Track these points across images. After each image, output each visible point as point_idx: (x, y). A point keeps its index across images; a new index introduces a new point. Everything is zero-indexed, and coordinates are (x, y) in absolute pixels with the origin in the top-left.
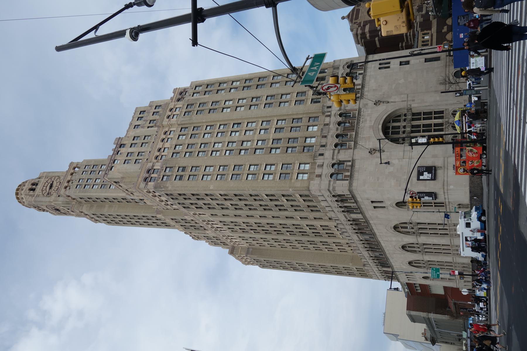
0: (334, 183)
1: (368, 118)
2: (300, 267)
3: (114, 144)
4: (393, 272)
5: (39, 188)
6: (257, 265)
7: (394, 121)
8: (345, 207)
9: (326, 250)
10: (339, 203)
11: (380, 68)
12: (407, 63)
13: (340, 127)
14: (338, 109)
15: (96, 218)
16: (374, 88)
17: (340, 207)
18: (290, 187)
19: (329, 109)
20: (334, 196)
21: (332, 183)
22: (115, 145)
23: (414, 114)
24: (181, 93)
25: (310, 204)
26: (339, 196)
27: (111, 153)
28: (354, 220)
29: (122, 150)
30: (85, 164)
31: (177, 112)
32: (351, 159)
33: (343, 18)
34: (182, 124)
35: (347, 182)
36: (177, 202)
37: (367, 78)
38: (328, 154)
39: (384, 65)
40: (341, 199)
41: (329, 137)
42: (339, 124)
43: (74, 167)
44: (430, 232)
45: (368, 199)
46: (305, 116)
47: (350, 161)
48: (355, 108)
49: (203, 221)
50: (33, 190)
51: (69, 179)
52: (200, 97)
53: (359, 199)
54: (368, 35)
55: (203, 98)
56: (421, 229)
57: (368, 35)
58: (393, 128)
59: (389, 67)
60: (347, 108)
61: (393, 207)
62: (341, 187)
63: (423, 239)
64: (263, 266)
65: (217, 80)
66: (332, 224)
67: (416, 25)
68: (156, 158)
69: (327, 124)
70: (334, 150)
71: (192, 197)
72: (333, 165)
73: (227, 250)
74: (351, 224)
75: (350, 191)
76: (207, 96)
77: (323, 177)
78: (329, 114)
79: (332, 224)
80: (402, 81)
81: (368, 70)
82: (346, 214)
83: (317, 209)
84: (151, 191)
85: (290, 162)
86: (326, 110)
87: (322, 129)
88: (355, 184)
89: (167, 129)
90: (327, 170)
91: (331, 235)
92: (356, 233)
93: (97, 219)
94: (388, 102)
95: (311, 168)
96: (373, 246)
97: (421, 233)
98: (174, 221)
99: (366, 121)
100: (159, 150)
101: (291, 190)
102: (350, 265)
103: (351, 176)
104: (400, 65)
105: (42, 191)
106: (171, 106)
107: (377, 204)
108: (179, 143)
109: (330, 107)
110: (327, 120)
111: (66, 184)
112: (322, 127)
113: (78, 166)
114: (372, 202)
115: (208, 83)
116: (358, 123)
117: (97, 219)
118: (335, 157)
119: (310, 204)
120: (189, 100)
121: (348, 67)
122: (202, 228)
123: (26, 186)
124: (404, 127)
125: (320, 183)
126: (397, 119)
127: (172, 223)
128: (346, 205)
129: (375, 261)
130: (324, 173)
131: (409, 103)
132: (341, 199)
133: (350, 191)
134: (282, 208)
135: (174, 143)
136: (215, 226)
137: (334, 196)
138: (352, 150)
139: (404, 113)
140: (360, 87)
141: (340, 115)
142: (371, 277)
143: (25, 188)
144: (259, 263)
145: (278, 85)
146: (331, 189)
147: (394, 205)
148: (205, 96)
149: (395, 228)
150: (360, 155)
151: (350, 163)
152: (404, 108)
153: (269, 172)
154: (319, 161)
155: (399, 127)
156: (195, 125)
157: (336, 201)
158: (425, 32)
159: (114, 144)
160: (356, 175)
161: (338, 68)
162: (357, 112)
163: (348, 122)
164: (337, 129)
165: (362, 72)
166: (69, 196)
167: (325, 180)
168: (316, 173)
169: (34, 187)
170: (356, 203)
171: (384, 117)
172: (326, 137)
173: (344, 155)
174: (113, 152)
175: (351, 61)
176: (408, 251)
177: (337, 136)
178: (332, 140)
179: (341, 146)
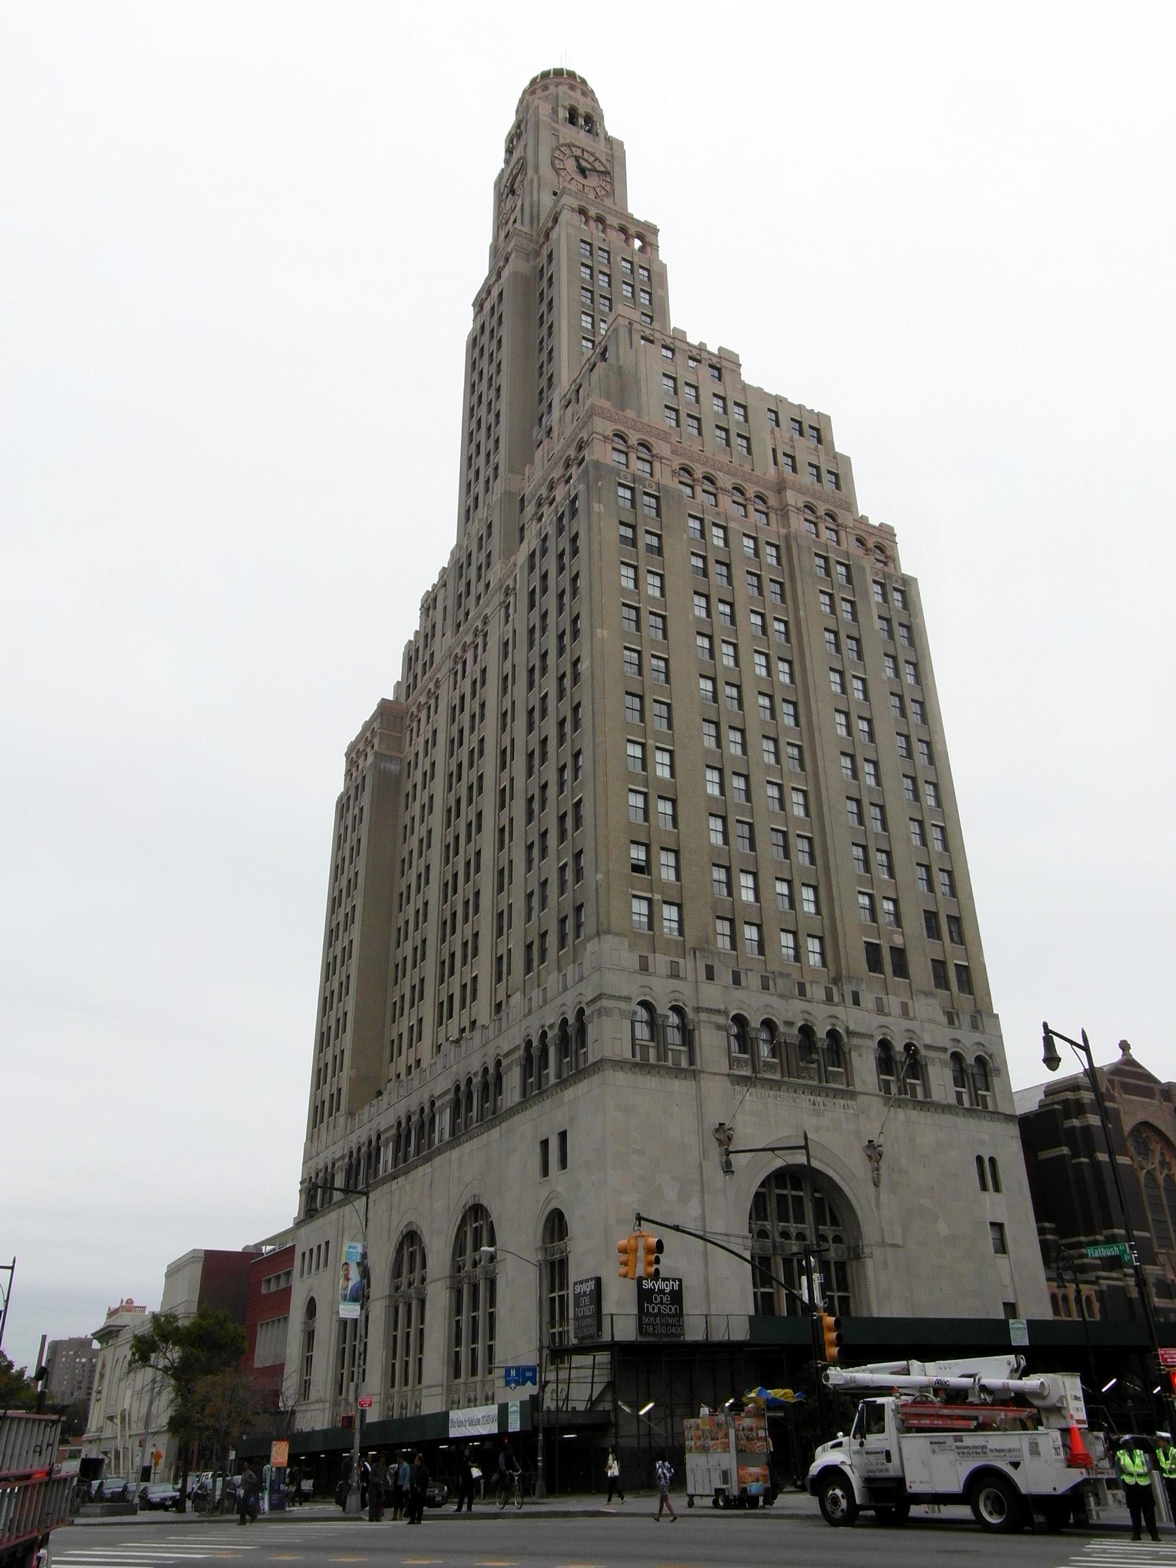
0: (622, 1013)
2: (341, 918)
3: (720, 349)
4: (328, 1203)
5: (579, 136)
6: (347, 790)
7: (818, 1204)
8: (544, 1050)
9: (397, 998)
10: (556, 1030)
11: (979, 1159)
12: (1001, 1247)
14: (851, 1028)
15: (487, 304)
17: (544, 1035)
18: (607, 874)
19: (849, 999)
20: (581, 1012)
21: (623, 1005)
22: (716, 352)
23: (841, 1266)
24: (880, 548)
25: (552, 940)
26: (582, 1030)
27: (693, 339)
28: (499, 1077)
29: (706, 373)
30: (655, 268)
31: (826, 535)
32: (698, 1066)
33: (1124, 1046)
34: (789, 548)
35: (628, 1055)
36: (551, 530)
37: (947, 1119)
38: (713, 995)
39: (988, 1173)
40: (572, 1035)
41: (766, 998)
43: (647, 234)
44: (464, 1319)
45: (572, 1120)
46: (827, 922)
47: (692, 1061)
48: (857, 1080)
49: (486, 617)
51: (608, 222)
52: (873, 605)
53: (570, 1093)
54: (1076, 1123)
56: (475, 1292)
57: (1076, 1123)
58: (798, 1201)
59: (984, 1188)
60: (854, 1054)
61: (548, 1200)
62: (611, 1037)
63: (438, 1297)
64: (343, 806)
65: (926, 655)
66: (482, 1009)
67: (1114, 1275)
68: (687, 470)
69: (802, 992)
70: (725, 1013)
71: (566, 576)
72: (678, 1010)
73: (391, 698)
74: (486, 1070)
75: (599, 1065)
76: (879, 624)
77: (641, 979)
78: (836, 999)
79: (482, 1009)
80: (943, 1228)
81: (972, 1123)
82: (522, 1052)
83: (535, 963)
84: (586, 452)
85: (683, 875)
86: (848, 989)
87: (788, 976)
88: (622, 1078)
89: (772, 501)
90: (662, 992)
91: (444, 1011)
92: (458, 1088)
93: (487, 306)
94: (876, 1184)
95: (668, 941)
96: (414, 1140)
97: (459, 1292)
98: (484, 532)
99: (818, 1114)
101: (599, 876)
102: (346, 1073)
103: (643, 1066)
104: (992, 1224)
105: (570, 146)
106: (844, 518)
107: (554, 1153)
108: (731, 538)
109: (856, 1001)
111: (592, 212)
112: (796, 976)
113: (649, 249)
114: (563, 1135)
115: (914, 629)
116: (812, 1090)
117: (487, 306)
118: (703, 1016)
119: (552, 940)
120: (863, 569)
121: (979, 1059)
122: (461, 617)
123: (582, 99)
124: (801, 1236)
125: (623, 970)
126: (824, 1215)
127: (477, 528)
128: (552, 1051)
129: (364, 1149)
130: (654, 982)
131: (877, 1251)
132: (572, 1035)
133: (599, 1065)
134: (536, 852)
136: (469, 656)
137: (581, 1012)
138: (726, 1070)
139: (843, 1235)
141: (833, 1034)
142: (311, 1137)
143: (577, 94)
144: (352, 792)
145: (916, 840)
146: (605, 1003)
147: (554, 1205)
148: (876, 617)
149: (476, 1211)
150: (717, 1096)
151: (684, 1064)
152: (859, 1234)
153: (651, 811)
155: (800, 1219)
156: (787, 586)
157: (565, 1021)
158: (1096, 1306)
159: (720, 349)
160: (651, 1082)
161: (975, 1027)
163: (814, 1057)
164: (789, 1024)
165: (967, 1104)
166: (556, 221)
167: (632, 987)
168: (651, 957)
169: (581, 121)
170: (557, 1085)
171: (830, 1172)
172: (765, 987)
173: (713, 1043)
174: (696, 343)
175: (998, 1070)
176: (399, 1250)
177: (768, 1024)
178: (755, 1004)
179: (737, 1037)
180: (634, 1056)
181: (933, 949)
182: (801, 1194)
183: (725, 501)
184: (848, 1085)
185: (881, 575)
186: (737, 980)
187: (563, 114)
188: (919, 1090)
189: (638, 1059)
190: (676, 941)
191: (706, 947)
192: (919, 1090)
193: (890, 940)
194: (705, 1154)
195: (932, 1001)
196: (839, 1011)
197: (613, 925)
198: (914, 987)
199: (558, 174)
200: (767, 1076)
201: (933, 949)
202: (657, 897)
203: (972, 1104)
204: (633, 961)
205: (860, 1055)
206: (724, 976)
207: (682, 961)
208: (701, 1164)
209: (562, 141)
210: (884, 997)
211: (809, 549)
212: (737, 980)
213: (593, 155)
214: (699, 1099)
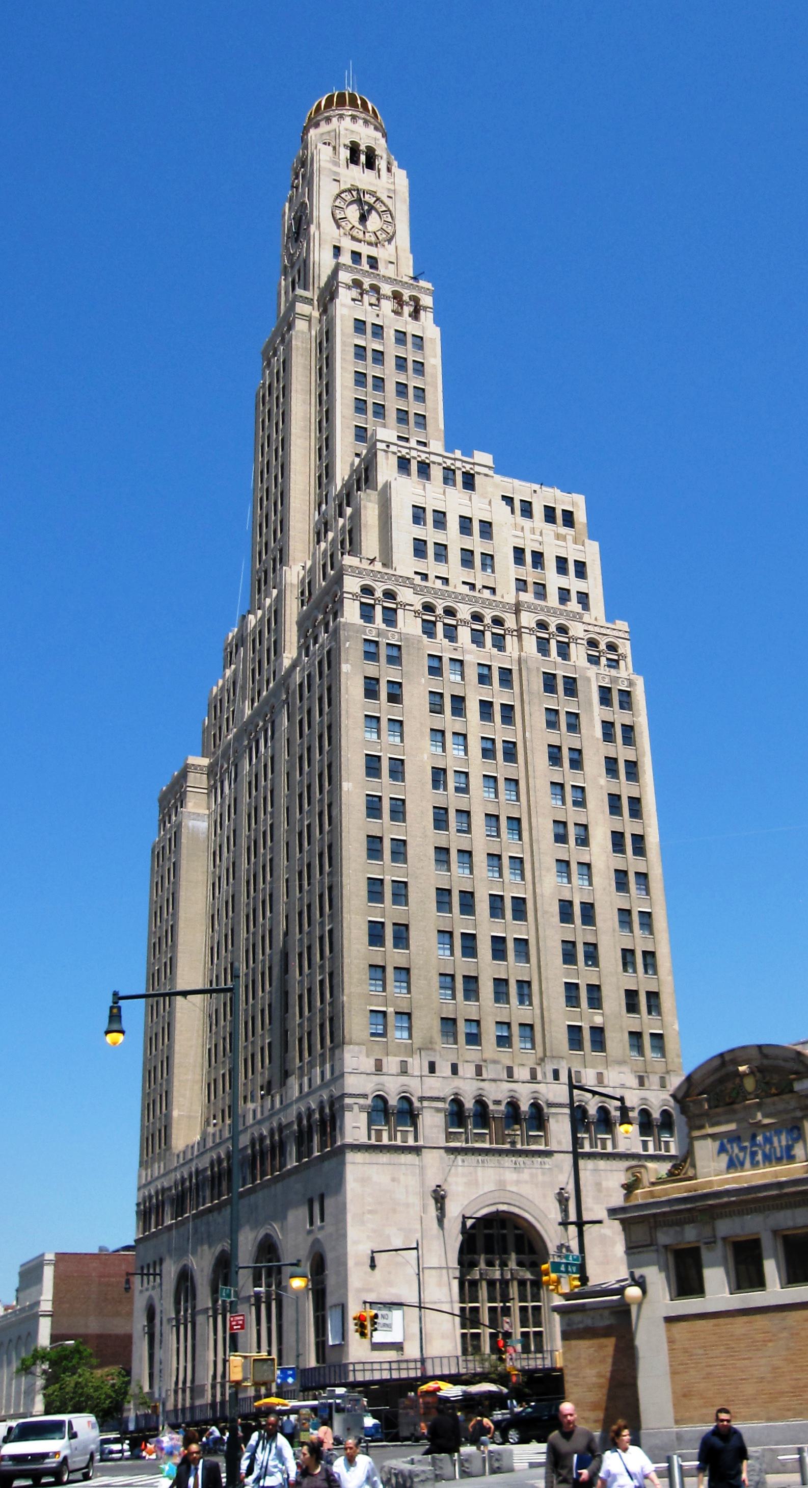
0: (362, 1108)
1: (525, 1175)
13: (502, 1107)
16: (605, 1184)
19: (550, 1076)
21: (361, 1101)
42: (513, 1105)
46: (537, 1011)
47: (416, 1140)
50: (354, 159)
55: (591, 719)
78: (539, 1077)
86: (549, 1067)
90: (393, 1088)
100: (450, 612)
110: (522, 1073)
111: (367, 282)
118: (425, 1104)
120: (588, 680)
135: (467, 658)
140: (609, 1149)
141: (536, 1106)
154: (417, 1065)
162: (542, 1147)
164: (497, 1102)
169: (363, 158)
173: (432, 1124)
180: (369, 1138)
181: (632, 1022)
182: (505, 1231)
183: (464, 634)
184: (546, 1145)
185: (607, 680)
186: (455, 1069)
187: (345, 154)
188: (609, 1144)
189: (373, 1141)
190: (406, 1045)
191: (430, 1046)
192: (609, 1144)
193: (592, 1021)
194: (424, 1209)
195: (626, 1069)
196: (541, 1088)
197: (354, 1037)
198: (610, 1059)
199: (339, 226)
200: (477, 1145)
201: (632, 1022)
202: (390, 1010)
203: (655, 1150)
204: (368, 1064)
205: (557, 1121)
206: (444, 1069)
207: (410, 1060)
208: (421, 1217)
209: (343, 187)
210: (583, 1071)
211: (538, 669)
212: (455, 1069)
213: (373, 193)
214: (422, 1168)
